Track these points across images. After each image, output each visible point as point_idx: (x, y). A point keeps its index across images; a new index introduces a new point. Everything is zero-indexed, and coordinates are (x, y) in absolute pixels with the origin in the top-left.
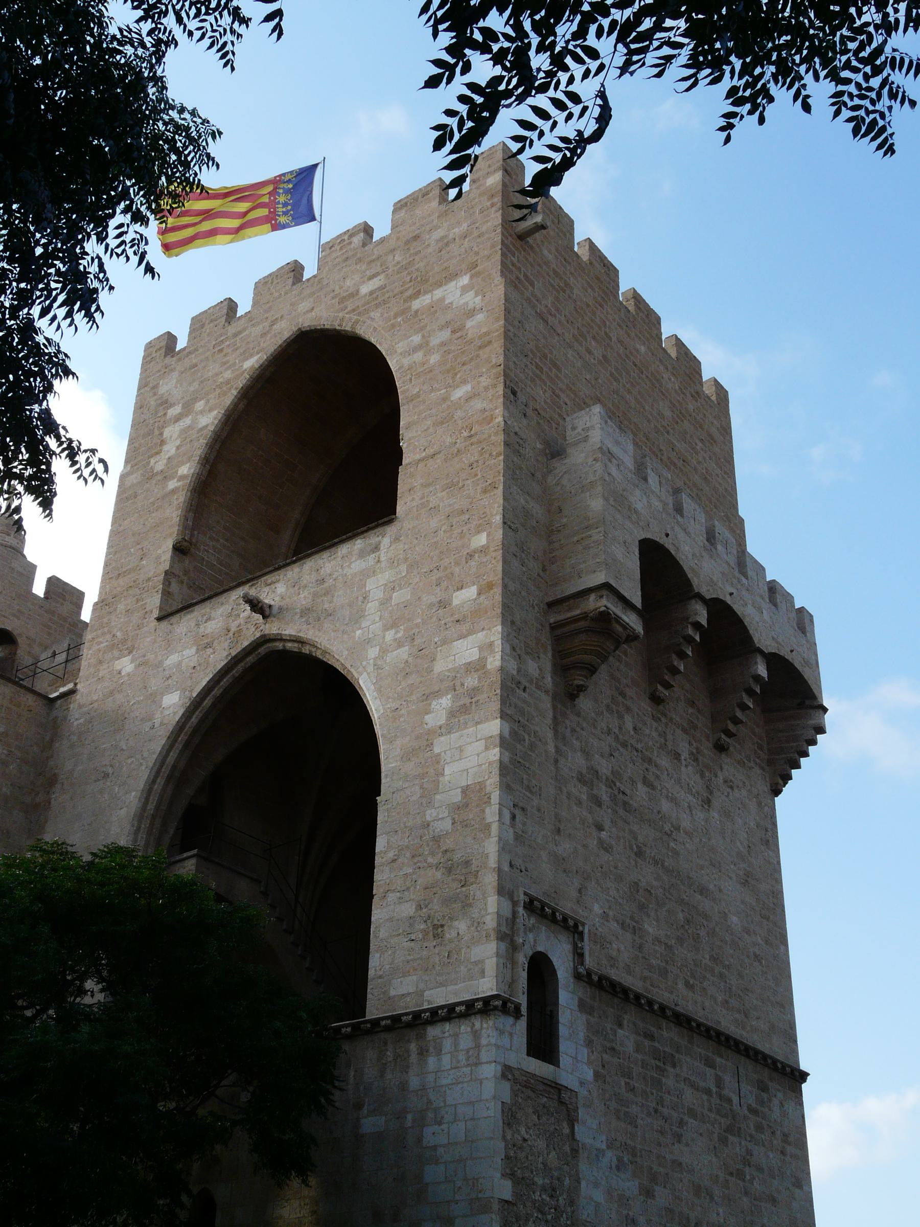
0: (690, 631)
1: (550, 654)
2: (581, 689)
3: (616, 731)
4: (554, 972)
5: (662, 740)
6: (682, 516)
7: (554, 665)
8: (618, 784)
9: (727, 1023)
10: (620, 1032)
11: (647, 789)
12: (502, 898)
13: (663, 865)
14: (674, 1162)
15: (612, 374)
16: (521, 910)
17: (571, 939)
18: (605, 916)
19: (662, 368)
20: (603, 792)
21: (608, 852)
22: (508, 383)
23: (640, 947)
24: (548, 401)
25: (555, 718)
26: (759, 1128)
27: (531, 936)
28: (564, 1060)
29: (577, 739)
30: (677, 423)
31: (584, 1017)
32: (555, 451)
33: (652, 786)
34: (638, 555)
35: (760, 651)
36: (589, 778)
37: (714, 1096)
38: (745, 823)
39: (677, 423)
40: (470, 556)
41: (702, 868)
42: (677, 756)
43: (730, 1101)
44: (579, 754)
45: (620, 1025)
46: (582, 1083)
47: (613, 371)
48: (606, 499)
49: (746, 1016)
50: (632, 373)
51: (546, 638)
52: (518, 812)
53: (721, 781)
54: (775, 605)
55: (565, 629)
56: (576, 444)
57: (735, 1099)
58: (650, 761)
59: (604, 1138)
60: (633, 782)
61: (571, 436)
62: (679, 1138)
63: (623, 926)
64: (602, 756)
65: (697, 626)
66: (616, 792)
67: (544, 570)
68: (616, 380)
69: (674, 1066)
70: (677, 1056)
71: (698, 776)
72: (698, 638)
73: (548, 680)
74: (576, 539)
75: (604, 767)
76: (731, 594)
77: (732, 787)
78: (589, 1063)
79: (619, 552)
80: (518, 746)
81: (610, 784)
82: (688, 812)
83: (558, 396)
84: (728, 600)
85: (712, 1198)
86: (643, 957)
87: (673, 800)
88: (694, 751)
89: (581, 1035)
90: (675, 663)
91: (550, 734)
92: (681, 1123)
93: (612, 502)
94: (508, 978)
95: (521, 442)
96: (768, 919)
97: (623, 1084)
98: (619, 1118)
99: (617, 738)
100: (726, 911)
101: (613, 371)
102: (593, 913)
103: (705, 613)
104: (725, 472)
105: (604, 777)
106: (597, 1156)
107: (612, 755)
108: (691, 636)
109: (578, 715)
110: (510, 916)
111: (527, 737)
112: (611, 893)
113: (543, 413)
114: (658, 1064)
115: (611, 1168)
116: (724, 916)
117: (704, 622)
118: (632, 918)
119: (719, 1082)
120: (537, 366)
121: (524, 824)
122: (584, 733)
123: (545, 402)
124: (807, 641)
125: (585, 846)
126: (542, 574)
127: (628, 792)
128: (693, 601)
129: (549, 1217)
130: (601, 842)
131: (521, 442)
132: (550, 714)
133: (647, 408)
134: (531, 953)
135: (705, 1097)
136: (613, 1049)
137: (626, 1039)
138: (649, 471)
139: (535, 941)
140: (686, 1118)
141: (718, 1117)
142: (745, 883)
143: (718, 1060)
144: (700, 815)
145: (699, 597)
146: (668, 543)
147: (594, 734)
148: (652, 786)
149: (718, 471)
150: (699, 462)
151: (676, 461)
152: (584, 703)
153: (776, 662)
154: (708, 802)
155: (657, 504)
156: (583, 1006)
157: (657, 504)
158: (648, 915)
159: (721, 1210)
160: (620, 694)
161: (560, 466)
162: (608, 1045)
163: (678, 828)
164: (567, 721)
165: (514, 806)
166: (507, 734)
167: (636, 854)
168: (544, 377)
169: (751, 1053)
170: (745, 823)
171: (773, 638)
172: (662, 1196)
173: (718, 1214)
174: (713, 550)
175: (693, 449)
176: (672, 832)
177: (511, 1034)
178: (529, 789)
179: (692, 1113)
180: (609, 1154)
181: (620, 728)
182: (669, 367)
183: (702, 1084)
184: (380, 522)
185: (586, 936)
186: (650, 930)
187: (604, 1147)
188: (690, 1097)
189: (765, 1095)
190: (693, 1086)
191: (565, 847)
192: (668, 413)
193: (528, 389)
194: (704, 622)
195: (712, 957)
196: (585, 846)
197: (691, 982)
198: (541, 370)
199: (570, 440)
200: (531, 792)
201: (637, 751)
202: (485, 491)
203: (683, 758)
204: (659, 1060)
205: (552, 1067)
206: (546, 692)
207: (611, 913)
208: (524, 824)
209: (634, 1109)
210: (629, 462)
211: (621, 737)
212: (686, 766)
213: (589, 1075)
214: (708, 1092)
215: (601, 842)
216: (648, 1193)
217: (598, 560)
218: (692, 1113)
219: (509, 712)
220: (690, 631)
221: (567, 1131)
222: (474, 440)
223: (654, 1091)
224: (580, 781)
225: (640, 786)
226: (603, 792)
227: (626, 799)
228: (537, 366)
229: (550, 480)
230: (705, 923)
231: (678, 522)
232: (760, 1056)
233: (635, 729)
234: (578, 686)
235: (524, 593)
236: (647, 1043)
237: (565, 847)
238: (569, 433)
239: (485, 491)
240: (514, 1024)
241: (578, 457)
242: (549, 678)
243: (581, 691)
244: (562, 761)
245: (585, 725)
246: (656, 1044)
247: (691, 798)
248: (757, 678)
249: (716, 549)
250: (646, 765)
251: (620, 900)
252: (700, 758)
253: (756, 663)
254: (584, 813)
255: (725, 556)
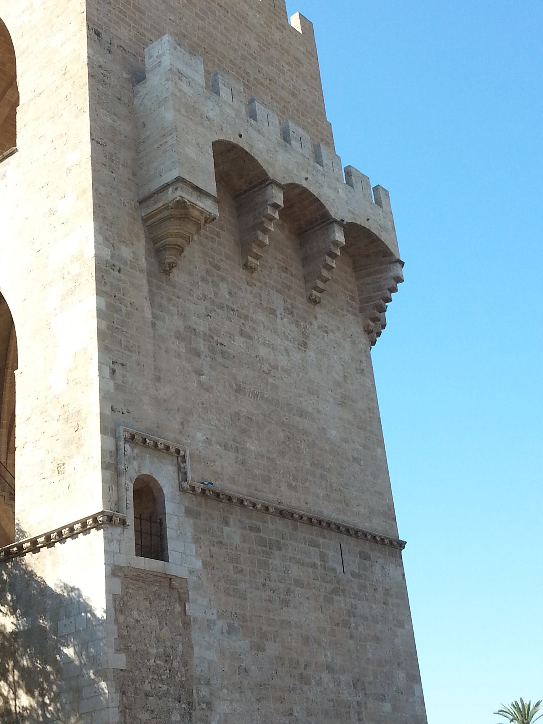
0: (270, 211)
1: (143, 242)
2: (172, 266)
3: (212, 296)
4: (161, 489)
5: (258, 301)
6: (255, 119)
7: (148, 250)
8: (215, 338)
9: (329, 512)
10: (226, 529)
11: (244, 339)
12: (105, 437)
13: (262, 397)
14: (282, 622)
15: (197, 15)
16: (122, 443)
17: (175, 461)
18: (208, 441)
19: (246, 7)
20: (202, 345)
21: (208, 391)
22: (91, 26)
23: (243, 463)
24: (134, 39)
25: (150, 291)
26: (363, 587)
27: (135, 463)
28: (172, 555)
29: (174, 305)
30: (264, 50)
31: (191, 521)
32: (138, 77)
33: (250, 338)
34: (211, 152)
35: (335, 221)
36: (188, 335)
37: (319, 568)
38: (341, 358)
39: (264, 50)
40: (69, 170)
41: (300, 396)
42: (273, 312)
43: (334, 570)
44: (176, 317)
45: (227, 523)
46: (191, 572)
47: (198, 11)
48: (178, 110)
49: (347, 505)
50: (217, 13)
51: (139, 229)
52: (118, 368)
53: (316, 328)
54: (352, 186)
55: (154, 220)
56: (153, 69)
57: (339, 569)
58: (246, 317)
59: (215, 611)
60: (231, 336)
61: (149, 63)
62: (286, 603)
63: (225, 447)
64: (199, 317)
65: (276, 206)
66: (214, 344)
67: (134, 174)
68: (202, 19)
69: (280, 549)
70: (282, 541)
71: (293, 326)
72: (277, 216)
73: (143, 262)
74: (156, 146)
75: (202, 326)
76: (306, 179)
77: (327, 332)
78: (198, 555)
79: (191, 152)
80: (116, 315)
81: (208, 338)
82: (285, 354)
83: (144, 35)
84: (304, 184)
85: (319, 644)
86: (246, 470)
87: (272, 347)
88: (289, 307)
89: (189, 534)
90: (261, 238)
91: (147, 304)
92: (288, 592)
93: (183, 111)
94: (114, 498)
95: (105, 73)
96: (365, 430)
97: (231, 568)
98: (228, 594)
99: (213, 302)
100: (325, 427)
101: (198, 11)
102: (197, 439)
103: (281, 195)
104: (312, 87)
105: (202, 334)
106: (209, 626)
107: (208, 315)
108: (271, 215)
109: (174, 287)
110: (113, 449)
111: (123, 308)
112: (213, 423)
113: (128, 49)
114: (265, 549)
115: (222, 633)
116: (324, 431)
117: (281, 203)
118: (234, 440)
119: (323, 557)
120: (120, 11)
121: (124, 376)
122: (180, 301)
123: (130, 40)
124: (383, 211)
125: (186, 389)
126: (132, 178)
127: (225, 343)
128: (270, 187)
129: (164, 677)
130: (201, 384)
131: (105, 73)
132: (146, 288)
133: (233, 40)
134: (136, 477)
135: (310, 570)
136: (220, 542)
137: (233, 533)
138: (221, 85)
139: (139, 467)
140: (292, 587)
141: (323, 584)
142: (342, 404)
143: (321, 540)
144: (296, 356)
145: (274, 182)
146: (242, 143)
147: (190, 301)
148: (250, 338)
149: (306, 87)
150: (286, 81)
151: (263, 81)
152: (177, 276)
153: (353, 230)
154: (305, 344)
155: (230, 112)
156: (189, 512)
157: (230, 112)
158: (250, 437)
159: (329, 654)
160: (214, 267)
161: (142, 89)
162: (216, 540)
163: (276, 368)
164: (163, 292)
165: (113, 363)
166: (103, 307)
167: (236, 391)
168: (127, 20)
169: (352, 532)
170: (341, 358)
171: (349, 211)
172: (272, 649)
173: (326, 656)
174: (288, 145)
175: (280, 70)
176: (270, 371)
177: (119, 542)
178: (127, 347)
179: (299, 583)
180: (220, 623)
181: (216, 294)
182: (254, 6)
183: (307, 560)
184: (5, 154)
185: (188, 458)
186: (252, 448)
187: (215, 617)
188: (295, 571)
189: (367, 563)
190: (300, 563)
191: (165, 391)
192: (254, 44)
193: (112, 30)
194: (281, 203)
195: (313, 464)
196: (186, 389)
197: (294, 484)
198: (125, 14)
199: (148, 66)
200: (130, 351)
201: (233, 310)
202: (77, 116)
203: (278, 312)
204: (266, 546)
205: (161, 562)
206: (142, 271)
207: (214, 439)
208: (124, 376)
209: (243, 586)
210: (200, 79)
211: (216, 301)
212: (282, 319)
213: (199, 564)
214: (314, 566)
215: (201, 384)
216: (260, 648)
217: (173, 160)
218: (299, 583)
219: (105, 289)
220: (270, 211)
221: (178, 608)
222: (67, 76)
223: (262, 570)
224: (178, 338)
225: (237, 337)
226: (202, 345)
227: (224, 348)
228: (120, 11)
229: (137, 102)
230: (305, 438)
231: (251, 125)
232: (360, 534)
233: (230, 293)
234: (169, 264)
235: (114, 194)
236: (253, 534)
237: (165, 391)
238: (147, 60)
239: (77, 116)
240: (123, 533)
241: (155, 80)
242: (144, 260)
243: (173, 267)
244: (159, 324)
245: (180, 294)
246: (262, 534)
247: (287, 343)
248: (336, 243)
249: (290, 144)
250: (242, 321)
251: (223, 428)
252: (295, 312)
253: (334, 231)
254: (184, 363)
255: (300, 150)
